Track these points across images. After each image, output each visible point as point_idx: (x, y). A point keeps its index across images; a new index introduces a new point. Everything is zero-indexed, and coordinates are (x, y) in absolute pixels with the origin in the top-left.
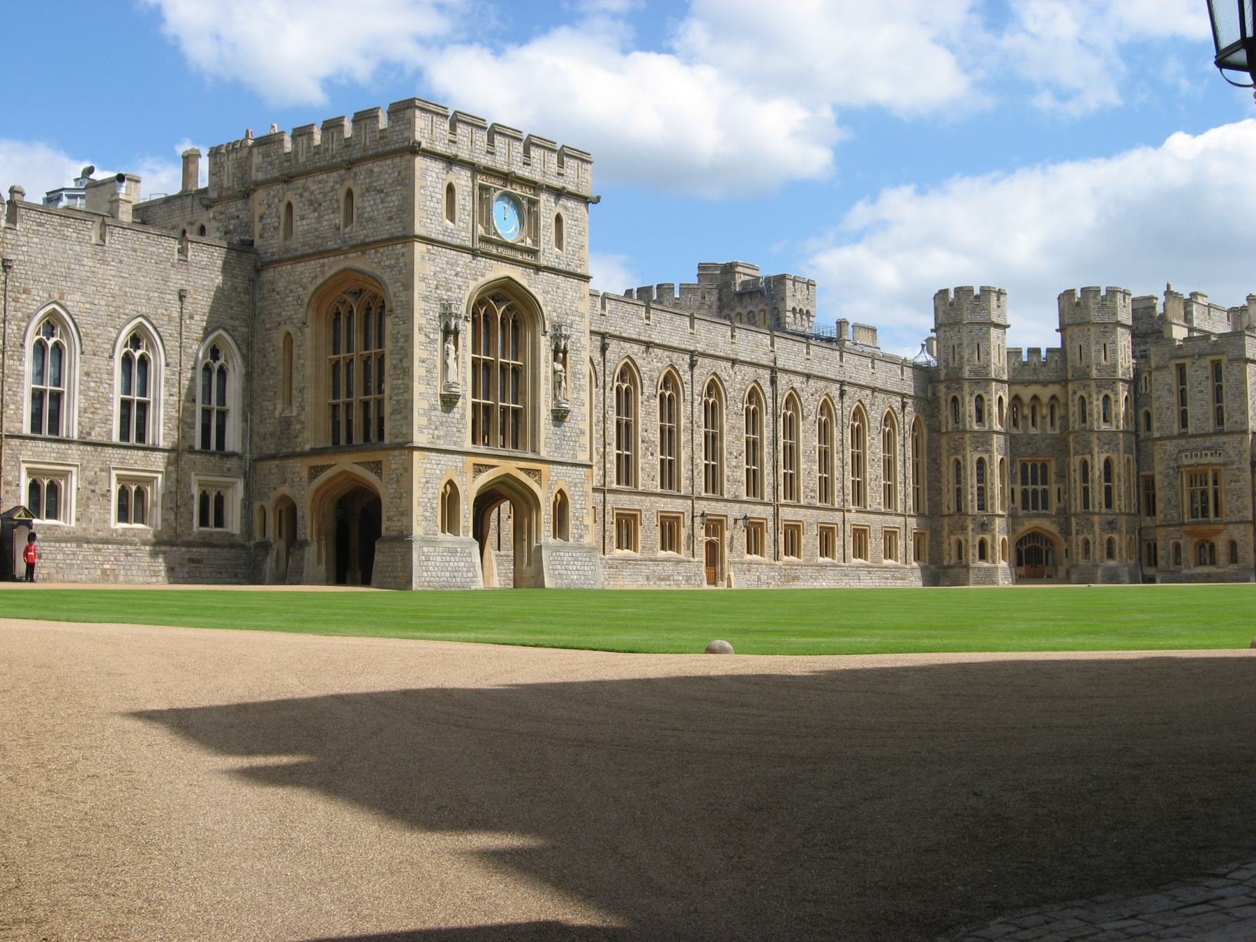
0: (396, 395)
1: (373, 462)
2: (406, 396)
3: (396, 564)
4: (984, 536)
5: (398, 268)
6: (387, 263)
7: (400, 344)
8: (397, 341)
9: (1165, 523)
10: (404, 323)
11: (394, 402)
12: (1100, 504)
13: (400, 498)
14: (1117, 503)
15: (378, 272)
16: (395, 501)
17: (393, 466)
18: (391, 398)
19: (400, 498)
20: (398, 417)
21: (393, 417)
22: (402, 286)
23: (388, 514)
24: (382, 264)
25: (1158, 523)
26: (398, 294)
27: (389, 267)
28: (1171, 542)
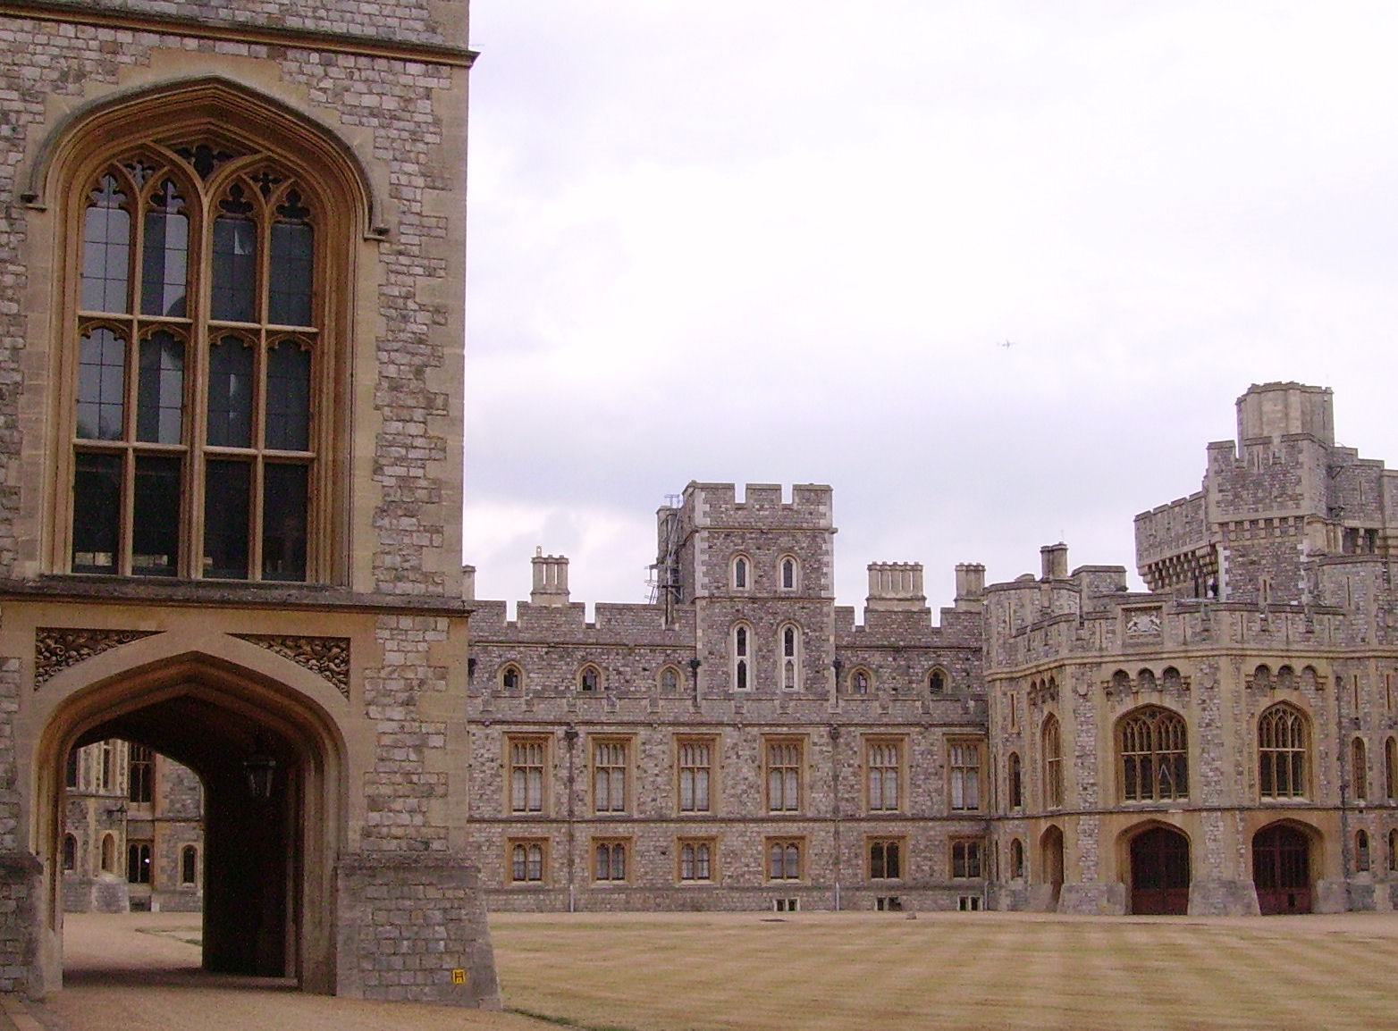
0: (399, 461)
1: (310, 640)
2: (433, 470)
3: (427, 933)
4: (110, 831)
5: (411, 126)
6: (369, 101)
7: (414, 328)
8: (405, 318)
9: (171, 815)
10: (431, 273)
11: (393, 482)
12: (98, 779)
13: (418, 748)
14: (119, 779)
15: (329, 119)
16: (399, 754)
17: (394, 658)
18: (378, 469)
19: (418, 748)
20: (406, 522)
21: (386, 522)
22: (423, 175)
23: (370, 790)
24: (349, 99)
25: (158, 815)
26: (407, 193)
27: (373, 113)
28: (181, 845)
